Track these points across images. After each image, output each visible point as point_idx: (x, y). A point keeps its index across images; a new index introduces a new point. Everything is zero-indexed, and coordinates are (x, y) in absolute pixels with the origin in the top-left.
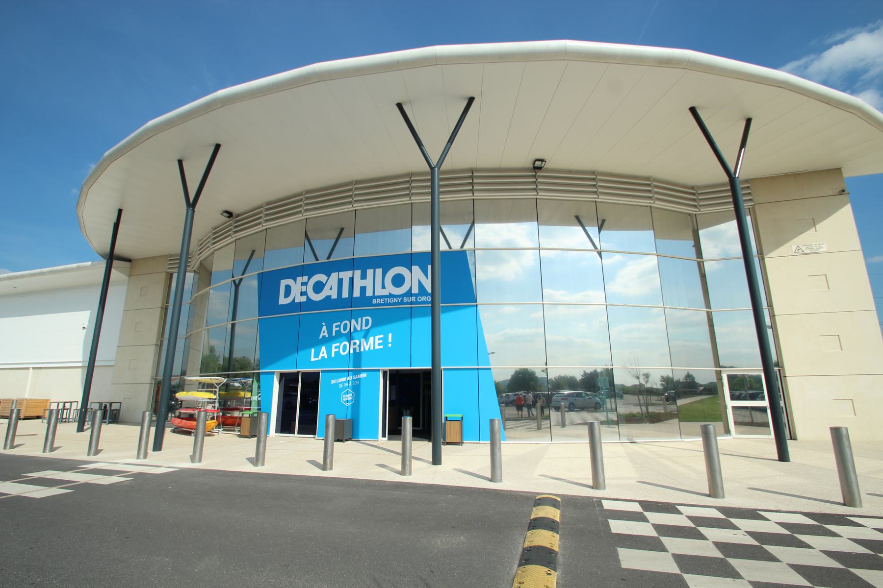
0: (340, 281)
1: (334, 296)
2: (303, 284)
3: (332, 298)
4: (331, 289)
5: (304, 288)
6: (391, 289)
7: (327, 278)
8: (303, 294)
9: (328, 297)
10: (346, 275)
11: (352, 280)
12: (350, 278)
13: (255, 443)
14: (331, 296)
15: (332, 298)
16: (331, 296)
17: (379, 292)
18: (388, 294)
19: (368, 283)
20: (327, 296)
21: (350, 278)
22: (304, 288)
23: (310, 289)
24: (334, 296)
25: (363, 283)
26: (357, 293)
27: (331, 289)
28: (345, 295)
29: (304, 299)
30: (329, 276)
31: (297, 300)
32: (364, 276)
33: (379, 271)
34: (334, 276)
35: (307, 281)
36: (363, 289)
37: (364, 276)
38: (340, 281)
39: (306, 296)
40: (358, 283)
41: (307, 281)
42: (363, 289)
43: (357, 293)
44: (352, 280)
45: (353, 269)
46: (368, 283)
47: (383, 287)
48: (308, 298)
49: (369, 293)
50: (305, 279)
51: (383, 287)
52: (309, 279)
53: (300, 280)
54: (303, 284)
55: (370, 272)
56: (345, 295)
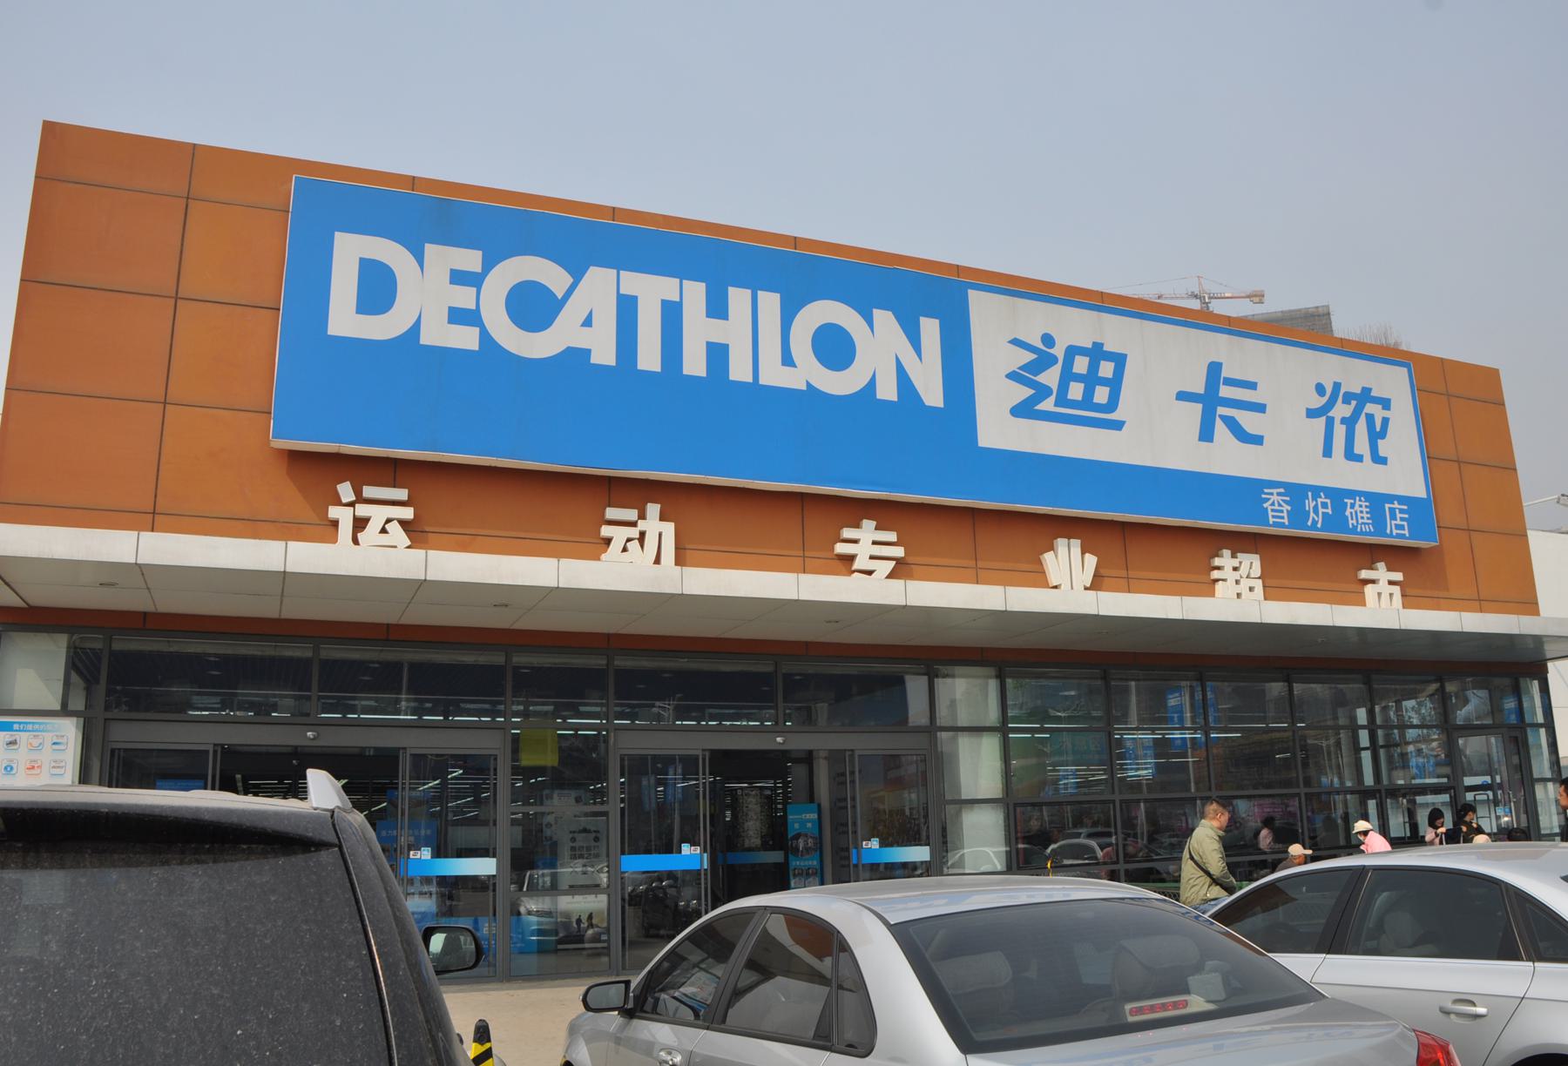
0: (627, 308)
1: (604, 353)
2: (458, 277)
3: (593, 361)
4: (588, 322)
5: (464, 297)
6: (808, 373)
7: (571, 280)
8: (458, 316)
9: (574, 357)
10: (651, 290)
11: (672, 314)
12: (665, 304)
13: (1383, 850)
14: (588, 352)
15: (592, 361)
16: (588, 352)
17: (774, 375)
18: (804, 388)
19: (734, 332)
20: (570, 351)
21: (665, 304)
22: (464, 297)
23: (493, 300)
24: (604, 353)
25: (717, 331)
26: (694, 364)
27: (588, 322)
28: (649, 358)
29: (465, 339)
30: (577, 275)
31: (440, 334)
32: (717, 308)
33: (770, 302)
34: (599, 287)
35: (478, 269)
36: (718, 354)
37: (717, 308)
38: (627, 308)
39: (478, 329)
40: (698, 331)
41: (478, 269)
42: (718, 354)
43: (694, 364)
44: (672, 314)
45: (682, 272)
46: (734, 332)
47: (788, 360)
48: (485, 336)
49: (739, 371)
50: (470, 260)
51: (788, 360)
52: (488, 265)
53: (444, 258)
54: (458, 277)
55: (738, 298)
56: (649, 358)
